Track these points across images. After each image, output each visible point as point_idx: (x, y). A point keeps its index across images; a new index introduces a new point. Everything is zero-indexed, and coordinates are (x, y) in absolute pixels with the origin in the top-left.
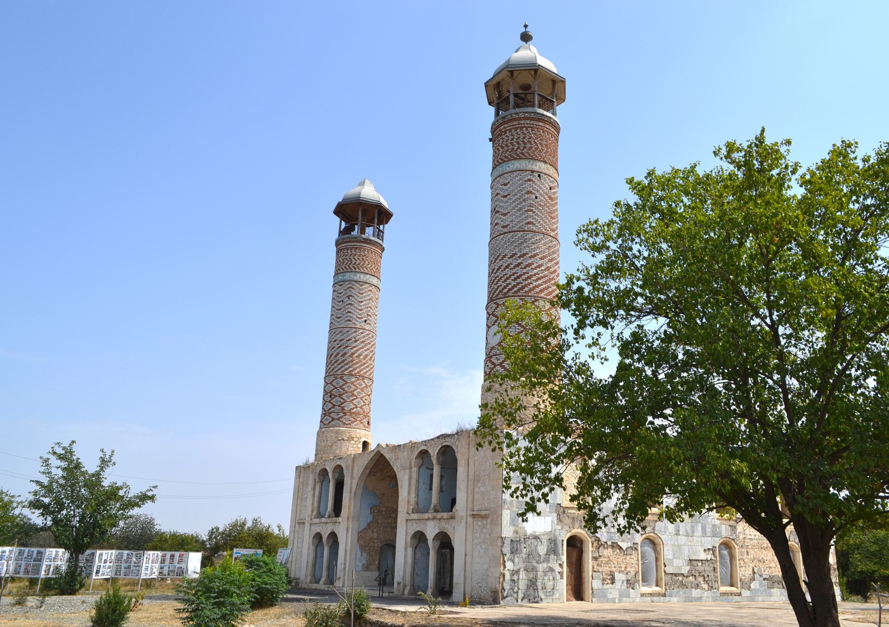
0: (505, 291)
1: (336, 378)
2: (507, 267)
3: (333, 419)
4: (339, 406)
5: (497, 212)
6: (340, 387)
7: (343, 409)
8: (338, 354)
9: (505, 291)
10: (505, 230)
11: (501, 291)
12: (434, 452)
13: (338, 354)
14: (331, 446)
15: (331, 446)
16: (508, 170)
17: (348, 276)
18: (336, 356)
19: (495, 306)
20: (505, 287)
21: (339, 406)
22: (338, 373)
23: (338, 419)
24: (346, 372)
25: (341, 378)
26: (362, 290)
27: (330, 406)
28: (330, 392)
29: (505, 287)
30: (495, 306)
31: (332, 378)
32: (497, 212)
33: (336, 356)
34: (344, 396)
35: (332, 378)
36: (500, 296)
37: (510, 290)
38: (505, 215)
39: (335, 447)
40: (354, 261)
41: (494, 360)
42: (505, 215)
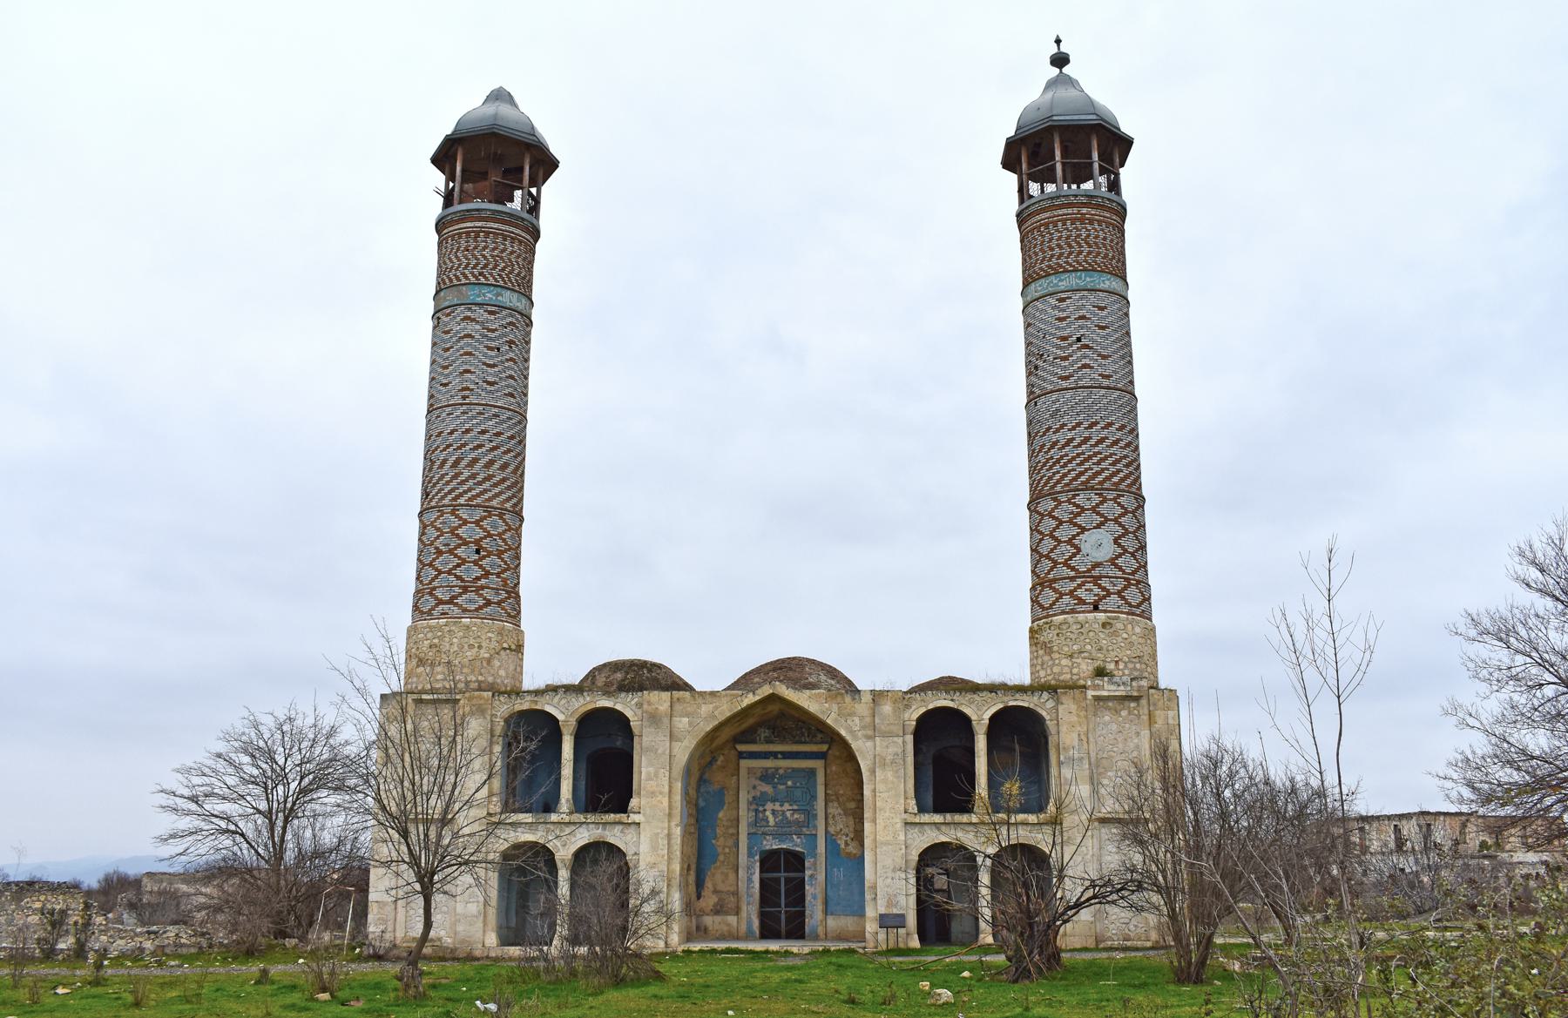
0: (1115, 479)
2: (1115, 443)
3: (488, 603)
4: (498, 575)
5: (1087, 347)
6: (499, 535)
7: (505, 584)
8: (491, 462)
9: (1115, 479)
10: (1106, 383)
11: (1108, 478)
12: (980, 713)
13: (491, 462)
14: (489, 661)
15: (489, 661)
16: (1102, 286)
19: (1097, 499)
20: (1114, 474)
21: (498, 575)
22: (494, 503)
23: (499, 603)
25: (501, 516)
28: (477, 542)
29: (1114, 474)
30: (1097, 499)
31: (479, 513)
32: (1087, 347)
34: (505, 556)
35: (479, 513)
36: (1106, 485)
37: (1122, 480)
38: (1104, 357)
39: (496, 663)
41: (1104, 583)
42: (1104, 357)
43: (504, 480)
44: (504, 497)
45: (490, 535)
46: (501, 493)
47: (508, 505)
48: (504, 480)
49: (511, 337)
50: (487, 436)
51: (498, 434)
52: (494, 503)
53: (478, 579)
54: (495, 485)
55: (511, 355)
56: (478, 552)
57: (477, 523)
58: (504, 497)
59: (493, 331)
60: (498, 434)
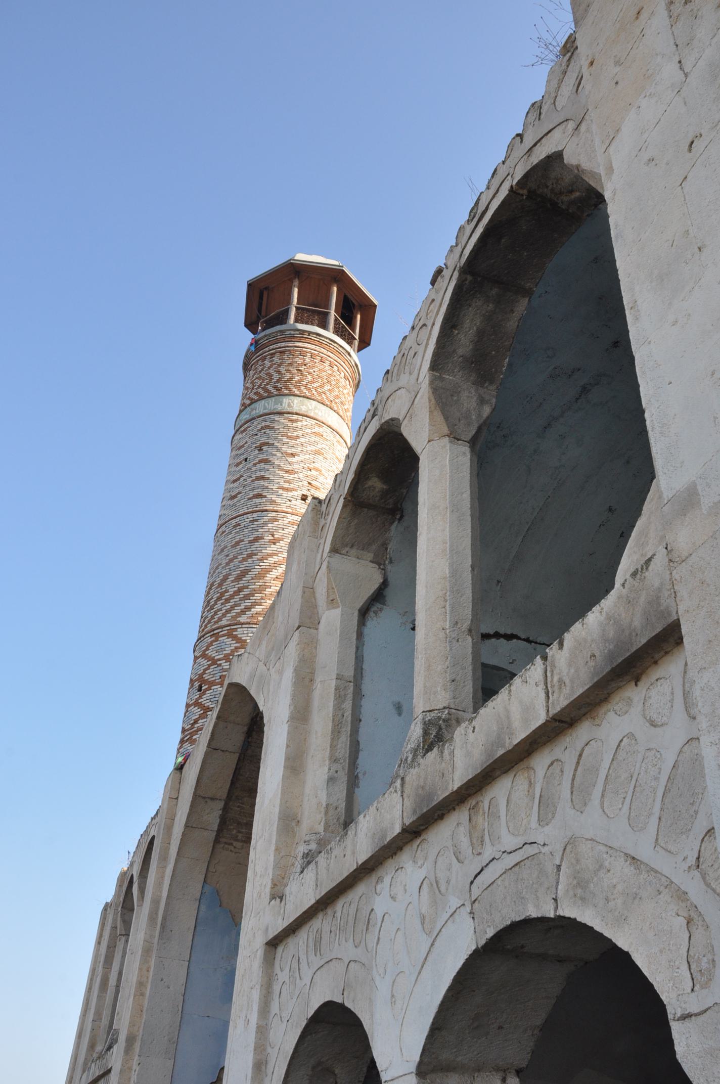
1: (217, 636)
8: (225, 578)
13: (225, 578)
17: (261, 407)
18: (220, 585)
22: (224, 622)
24: (243, 619)
25: (230, 635)
26: (295, 429)
27: (197, 711)
33: (220, 585)
40: (276, 377)
43: (240, 590)
44: (238, 609)
45: (214, 662)
46: (232, 608)
47: (243, 619)
48: (240, 590)
49: (263, 440)
50: (226, 552)
51: (237, 543)
52: (224, 622)
53: (196, 722)
54: (227, 601)
55: (261, 457)
56: (200, 689)
57: (204, 655)
58: (238, 609)
59: (243, 446)
60: (237, 543)
